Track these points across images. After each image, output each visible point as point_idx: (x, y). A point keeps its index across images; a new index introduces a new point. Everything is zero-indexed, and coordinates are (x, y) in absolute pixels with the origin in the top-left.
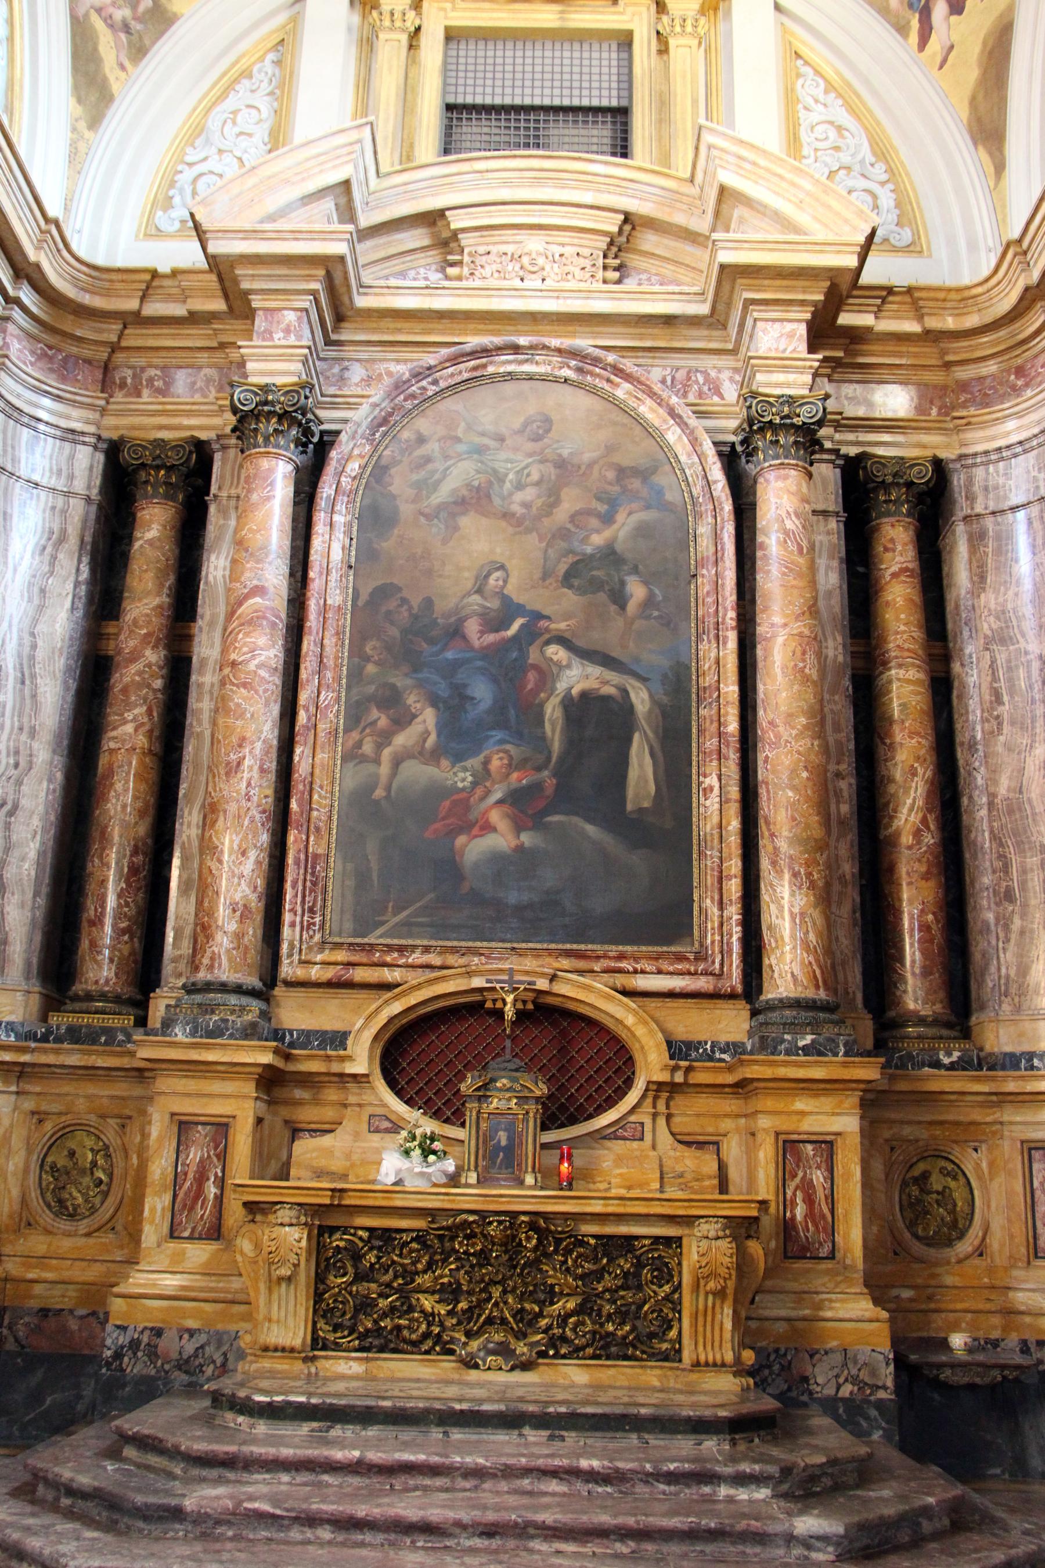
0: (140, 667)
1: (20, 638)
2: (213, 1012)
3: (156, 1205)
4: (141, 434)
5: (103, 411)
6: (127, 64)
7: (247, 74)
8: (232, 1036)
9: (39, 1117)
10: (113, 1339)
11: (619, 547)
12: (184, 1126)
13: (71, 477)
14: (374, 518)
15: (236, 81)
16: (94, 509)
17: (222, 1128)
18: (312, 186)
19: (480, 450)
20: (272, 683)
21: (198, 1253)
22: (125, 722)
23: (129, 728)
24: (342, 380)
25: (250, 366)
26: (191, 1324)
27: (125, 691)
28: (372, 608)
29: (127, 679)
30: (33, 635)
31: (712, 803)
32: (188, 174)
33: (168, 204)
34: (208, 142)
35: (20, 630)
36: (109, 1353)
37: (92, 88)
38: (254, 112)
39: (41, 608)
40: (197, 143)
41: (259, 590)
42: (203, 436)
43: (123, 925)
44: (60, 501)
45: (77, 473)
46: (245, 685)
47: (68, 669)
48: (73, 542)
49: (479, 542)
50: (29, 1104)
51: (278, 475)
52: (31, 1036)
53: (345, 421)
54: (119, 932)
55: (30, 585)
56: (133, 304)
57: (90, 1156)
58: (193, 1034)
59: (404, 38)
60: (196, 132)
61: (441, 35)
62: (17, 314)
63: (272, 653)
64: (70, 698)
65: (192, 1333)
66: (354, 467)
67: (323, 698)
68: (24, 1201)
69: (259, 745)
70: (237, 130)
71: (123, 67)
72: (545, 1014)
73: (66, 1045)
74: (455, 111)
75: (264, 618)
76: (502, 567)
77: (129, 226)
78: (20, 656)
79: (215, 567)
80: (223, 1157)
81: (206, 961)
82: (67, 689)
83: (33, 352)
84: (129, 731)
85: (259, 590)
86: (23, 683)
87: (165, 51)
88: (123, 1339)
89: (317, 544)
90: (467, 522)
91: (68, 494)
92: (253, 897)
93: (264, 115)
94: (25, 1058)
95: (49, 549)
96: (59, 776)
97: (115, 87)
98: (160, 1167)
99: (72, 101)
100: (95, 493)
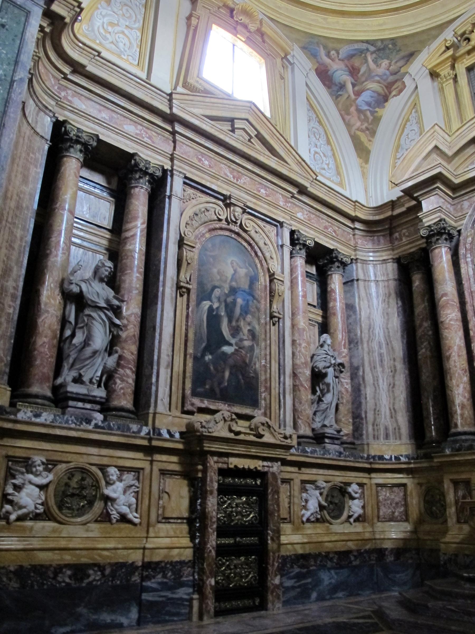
1: (384, 331)
2: (457, 443)
3: (452, 511)
4: (404, 253)
5: (393, 250)
6: (371, 139)
7: (408, 120)
8: (465, 450)
9: (420, 484)
10: (443, 558)
13: (388, 275)
15: (405, 124)
16: (398, 282)
18: (424, 154)
21: (466, 528)
22: (422, 349)
23: (424, 350)
25: (424, 220)
26: (467, 552)
27: (420, 338)
29: (420, 334)
30: (387, 329)
34: (402, 149)
35: (383, 328)
36: (442, 563)
37: (363, 152)
38: (413, 131)
39: (388, 320)
40: (399, 150)
41: (445, 295)
42: (424, 245)
43: (435, 416)
44: (386, 284)
45: (389, 273)
46: (446, 328)
47: (402, 336)
48: (393, 295)
50: (416, 481)
52: (413, 458)
53: (462, 225)
54: (435, 420)
55: (383, 313)
56: (389, 214)
57: (438, 497)
58: (452, 451)
59: (451, 81)
60: (398, 147)
61: (464, 71)
62: (357, 232)
63: (454, 315)
64: (404, 346)
65: (468, 556)
68: (421, 513)
69: (456, 348)
70: (410, 140)
71: (370, 141)
73: (423, 460)
75: (448, 303)
77: (385, 188)
78: (385, 337)
81: (453, 425)
82: (403, 342)
83: (366, 241)
84: (424, 351)
85: (445, 295)
86: (388, 344)
88: (446, 558)
89: (463, 271)
91: (388, 281)
92: (465, 401)
93: (416, 130)
94: (412, 466)
95: (386, 300)
96: (407, 372)
97: (370, 148)
98: (450, 497)
99: (358, 159)
100: (396, 277)
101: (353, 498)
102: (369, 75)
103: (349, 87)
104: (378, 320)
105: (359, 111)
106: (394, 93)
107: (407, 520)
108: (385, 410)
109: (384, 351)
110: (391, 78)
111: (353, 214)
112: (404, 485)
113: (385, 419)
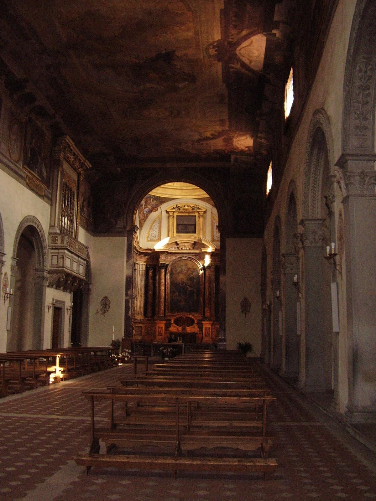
0: (151, 286)
7: (156, 221)
11: (194, 276)
12: (159, 327)
14: (172, 274)
17: (162, 328)
19: (181, 267)
20: (164, 291)
24: (168, 258)
28: (172, 283)
31: (201, 300)
32: (150, 233)
33: (149, 237)
49: (181, 276)
51: (163, 271)
60: (151, 228)
66: (170, 269)
67: (168, 291)
72: (187, 318)
74: (178, 225)
76: (183, 278)
79: (157, 277)
80: (162, 329)
87: (147, 220)
89: (167, 277)
90: (180, 274)
98: (157, 330)
101: (134, 329)
102: (149, 204)
103: (144, 205)
104: (139, 281)
105: (143, 213)
106: (154, 211)
107: (141, 335)
108: (138, 307)
109: (139, 291)
110: (155, 206)
111: (139, 251)
112: (141, 327)
113: (138, 310)
